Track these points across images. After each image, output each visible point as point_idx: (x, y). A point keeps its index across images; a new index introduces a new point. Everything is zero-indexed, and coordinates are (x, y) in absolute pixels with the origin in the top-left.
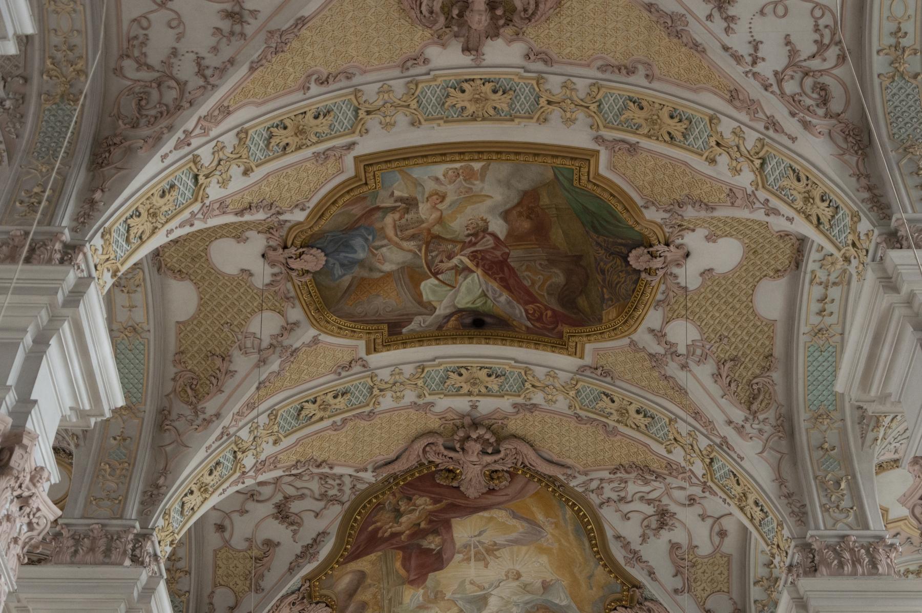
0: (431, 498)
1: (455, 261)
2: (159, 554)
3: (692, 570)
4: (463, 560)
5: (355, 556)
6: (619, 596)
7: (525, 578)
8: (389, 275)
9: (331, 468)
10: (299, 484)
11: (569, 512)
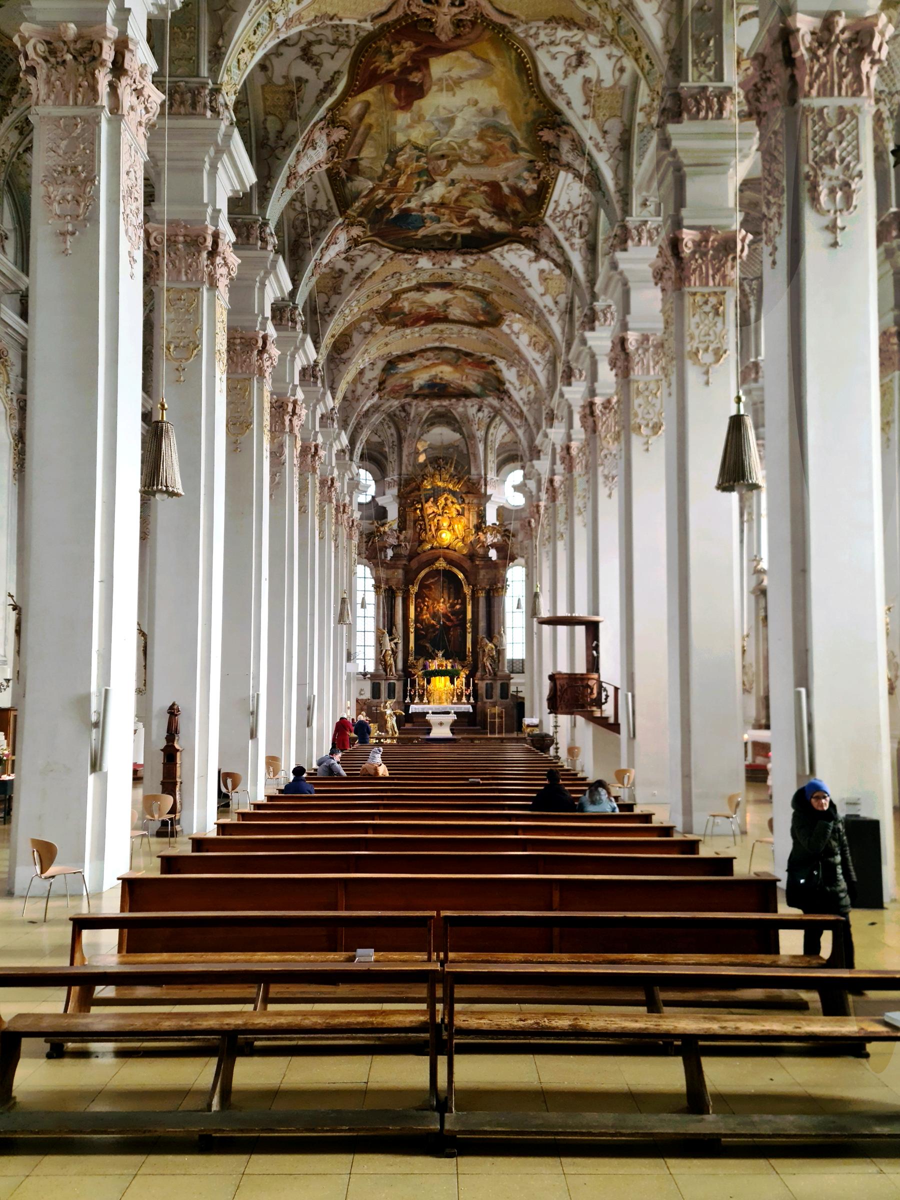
0: (414, 42)
2: (228, 103)
3: (598, 99)
4: (438, 91)
5: (363, 89)
6: (545, 119)
7: (481, 105)
9: (341, 20)
10: (317, 32)
11: (513, 54)
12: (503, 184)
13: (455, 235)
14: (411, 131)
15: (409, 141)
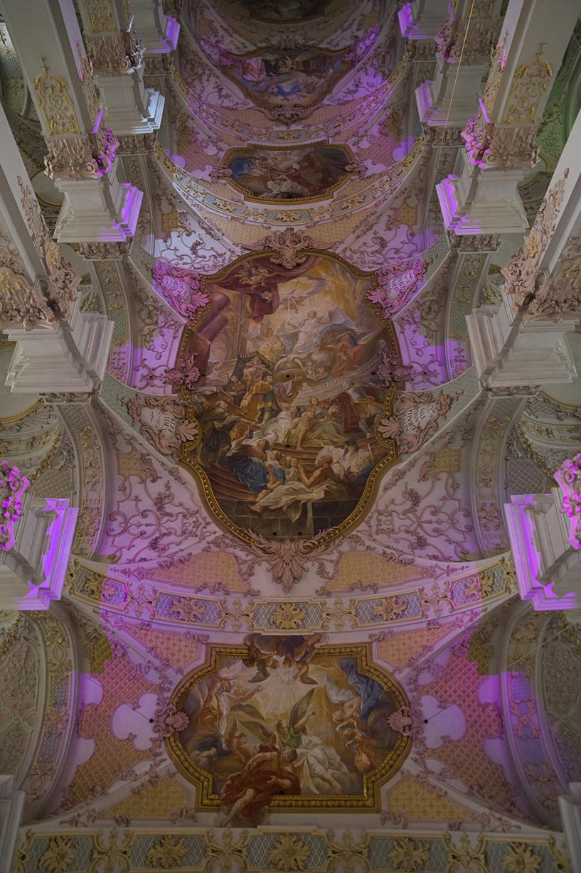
7: (319, 315)
12: (350, 392)
13: (305, 504)
14: (259, 343)
15: (258, 353)
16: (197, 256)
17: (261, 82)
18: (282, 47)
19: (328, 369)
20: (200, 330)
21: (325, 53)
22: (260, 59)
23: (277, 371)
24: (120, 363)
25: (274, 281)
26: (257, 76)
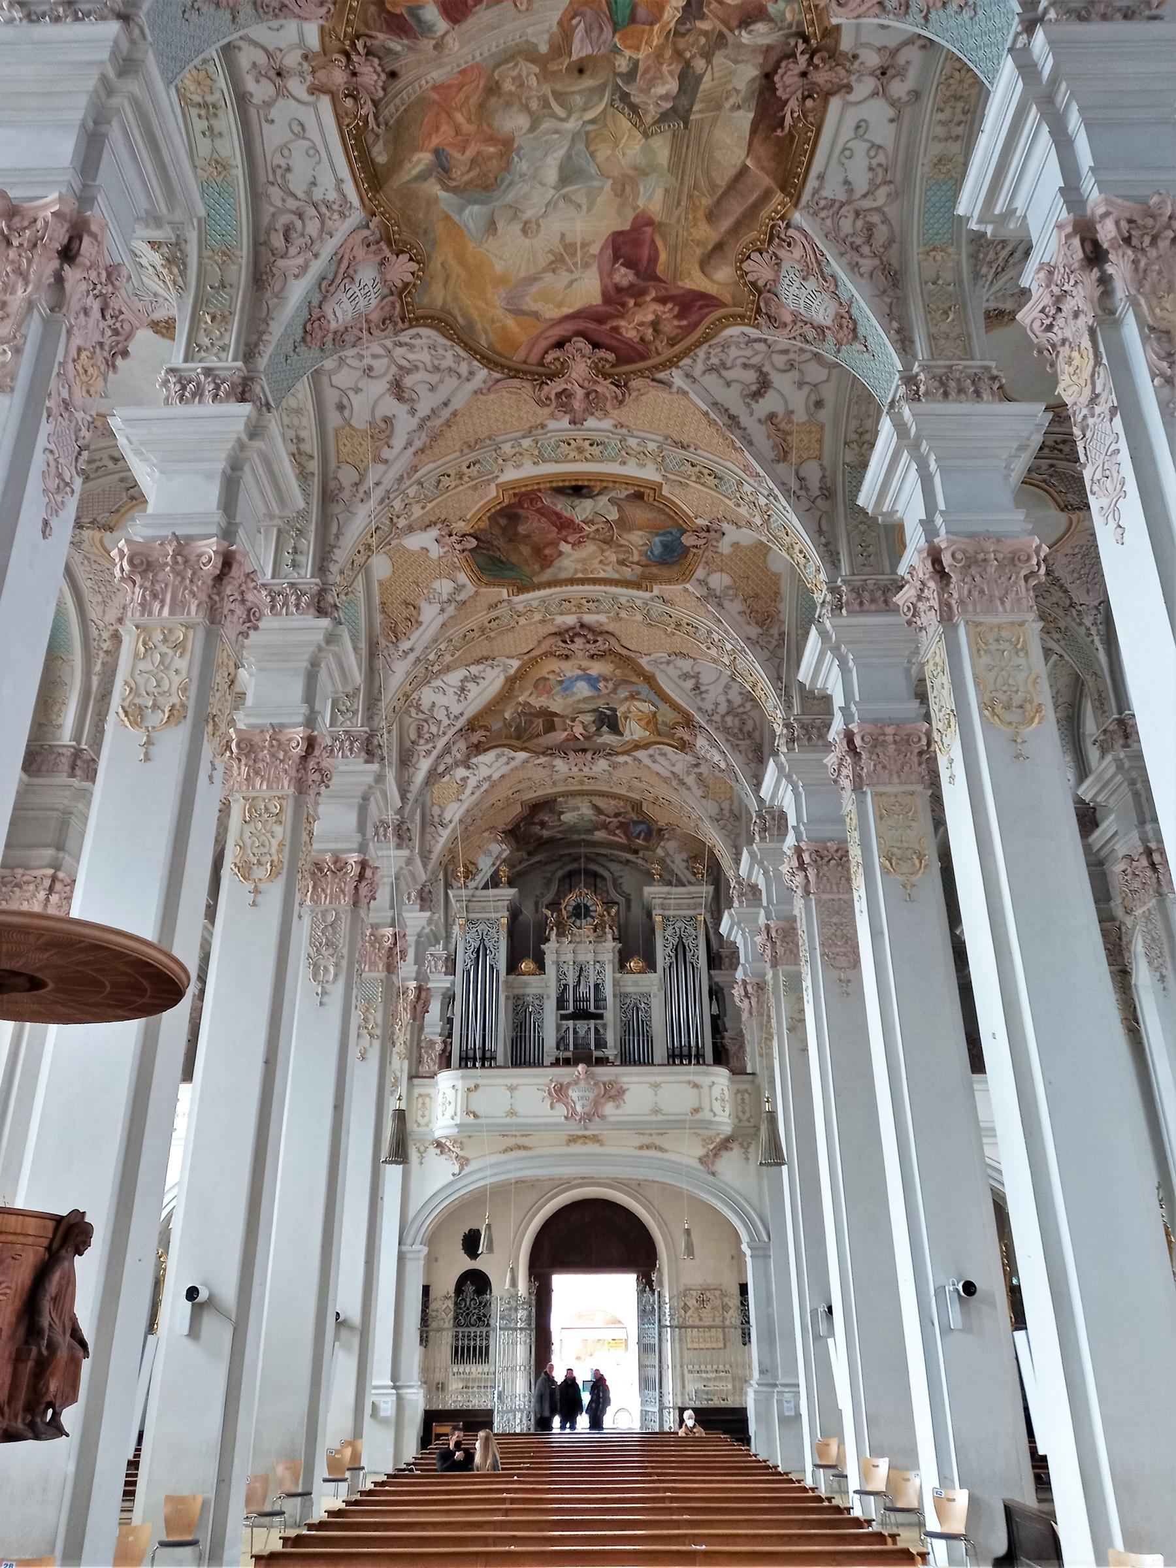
0: (621, 334)
1: (594, 528)
5: (704, 301)
8: (640, 529)
11: (483, 342)
12: (442, 25)
15: (646, 135)
16: (759, 369)
17: (626, 699)
18: (589, 755)
19: (493, 89)
20: (767, 195)
21: (518, 744)
22: (627, 737)
23: (603, 87)
24: (948, 111)
25: (609, 309)
26: (633, 709)
